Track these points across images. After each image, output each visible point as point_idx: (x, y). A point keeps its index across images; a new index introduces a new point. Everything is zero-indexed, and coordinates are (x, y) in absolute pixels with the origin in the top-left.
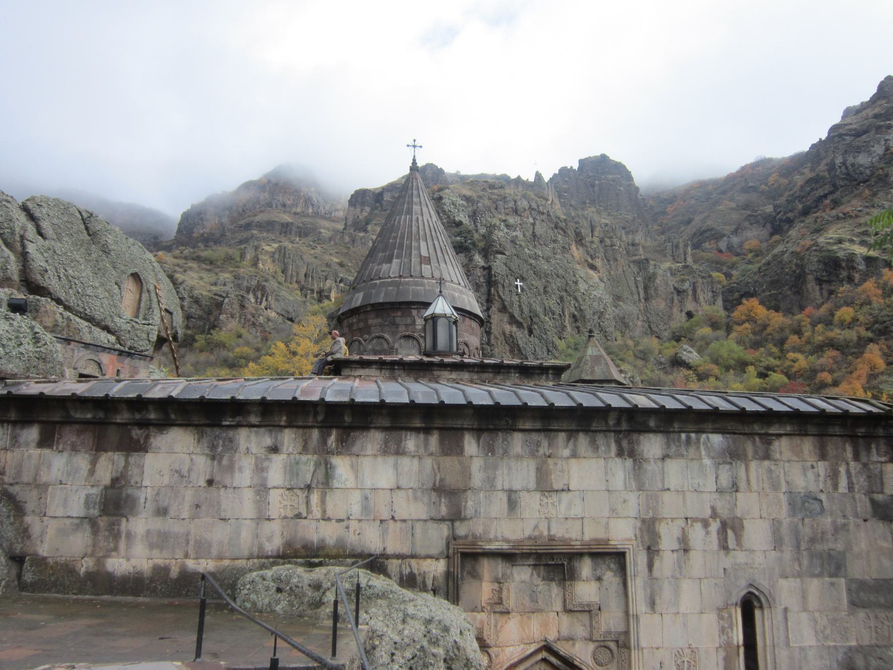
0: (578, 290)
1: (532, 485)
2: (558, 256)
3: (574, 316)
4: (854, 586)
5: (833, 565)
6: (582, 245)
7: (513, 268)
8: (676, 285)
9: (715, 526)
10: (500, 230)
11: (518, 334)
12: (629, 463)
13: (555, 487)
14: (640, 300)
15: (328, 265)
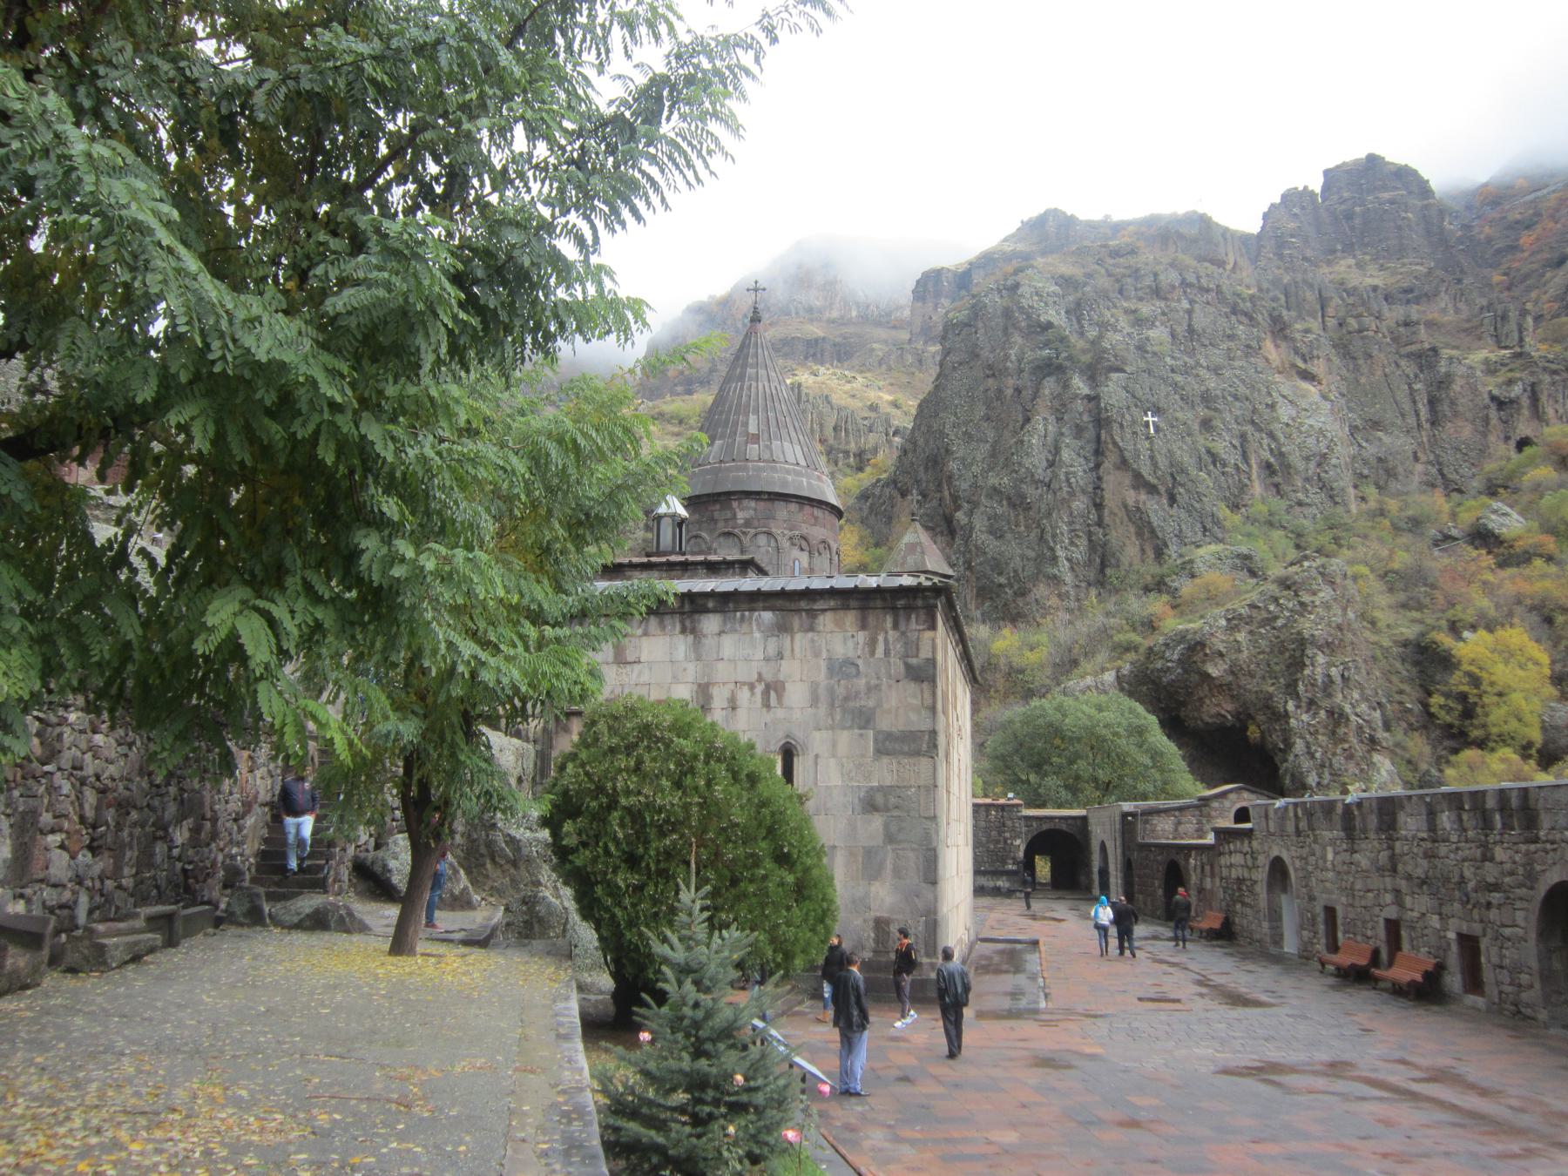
0: (1277, 419)
1: (611, 659)
2: (1237, 363)
3: (1268, 466)
4: (881, 737)
5: (864, 719)
6: (1285, 338)
7: (1139, 393)
8: (1496, 392)
9: (759, 688)
10: (1116, 331)
11: (1149, 504)
12: (690, 638)
13: (629, 659)
14: (1419, 425)
15: (873, 408)
